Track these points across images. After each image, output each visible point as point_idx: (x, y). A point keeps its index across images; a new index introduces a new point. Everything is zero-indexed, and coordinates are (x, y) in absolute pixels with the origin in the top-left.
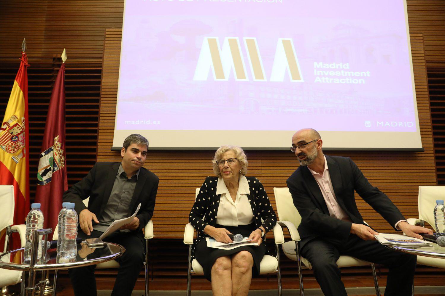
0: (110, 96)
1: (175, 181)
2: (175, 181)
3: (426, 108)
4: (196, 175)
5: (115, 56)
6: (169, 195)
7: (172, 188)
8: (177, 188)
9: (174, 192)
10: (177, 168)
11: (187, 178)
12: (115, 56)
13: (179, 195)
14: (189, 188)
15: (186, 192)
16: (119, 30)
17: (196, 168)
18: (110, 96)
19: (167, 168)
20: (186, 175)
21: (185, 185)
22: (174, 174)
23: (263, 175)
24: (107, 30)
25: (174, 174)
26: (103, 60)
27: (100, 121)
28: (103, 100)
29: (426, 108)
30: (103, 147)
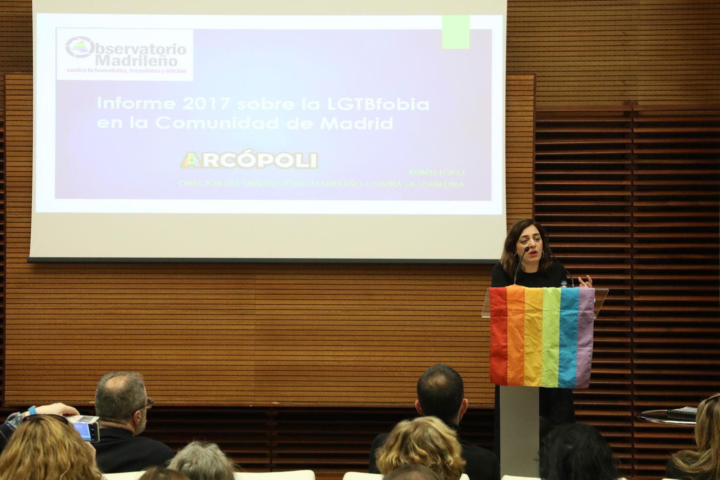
0: (20, 189)
1: (125, 322)
2: (125, 322)
3: (527, 206)
4: (157, 312)
5: (24, 123)
6: (117, 342)
7: (121, 332)
8: (128, 332)
9: (124, 337)
10: (128, 301)
11: (143, 317)
12: (24, 123)
13: (132, 342)
14: (147, 332)
15: (142, 337)
16: (28, 77)
17: (157, 301)
18: (20, 189)
19: (113, 301)
20: (143, 312)
21: (141, 327)
22: (124, 311)
23: (257, 312)
24: (7, 76)
25: (124, 311)
26: (5, 129)
27: (7, 229)
28: (9, 195)
29: (527, 206)
30: (13, 271)
